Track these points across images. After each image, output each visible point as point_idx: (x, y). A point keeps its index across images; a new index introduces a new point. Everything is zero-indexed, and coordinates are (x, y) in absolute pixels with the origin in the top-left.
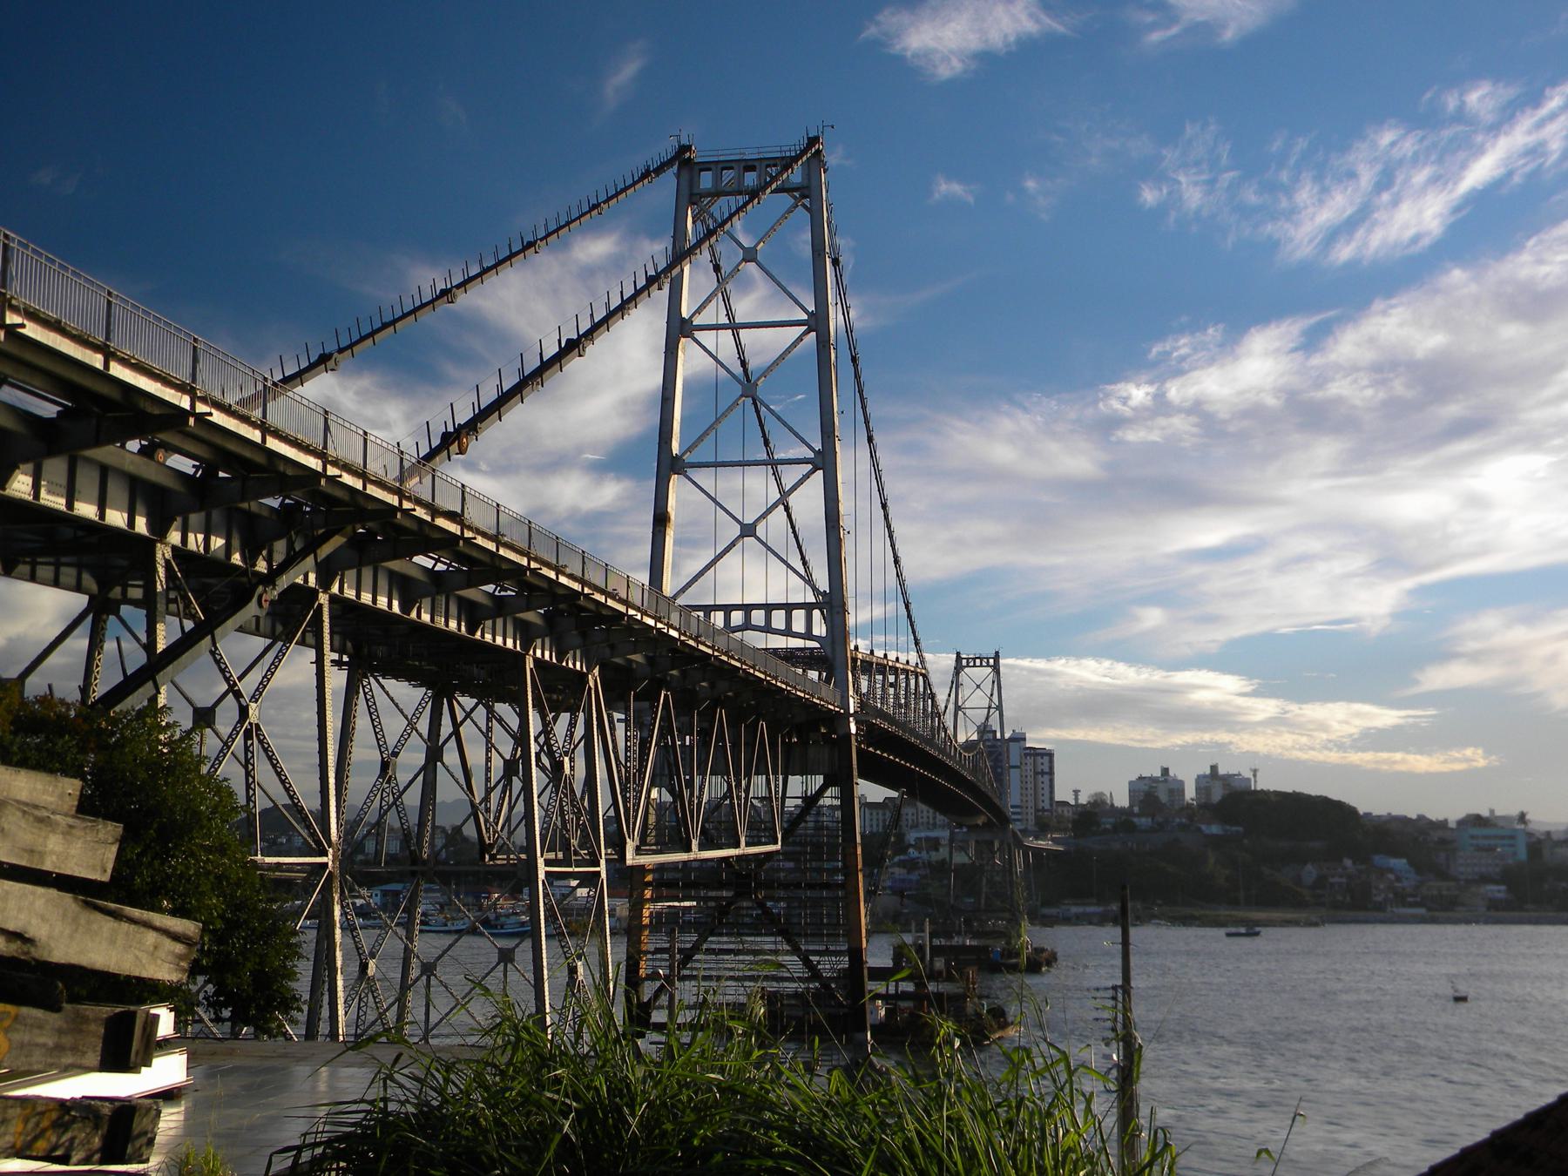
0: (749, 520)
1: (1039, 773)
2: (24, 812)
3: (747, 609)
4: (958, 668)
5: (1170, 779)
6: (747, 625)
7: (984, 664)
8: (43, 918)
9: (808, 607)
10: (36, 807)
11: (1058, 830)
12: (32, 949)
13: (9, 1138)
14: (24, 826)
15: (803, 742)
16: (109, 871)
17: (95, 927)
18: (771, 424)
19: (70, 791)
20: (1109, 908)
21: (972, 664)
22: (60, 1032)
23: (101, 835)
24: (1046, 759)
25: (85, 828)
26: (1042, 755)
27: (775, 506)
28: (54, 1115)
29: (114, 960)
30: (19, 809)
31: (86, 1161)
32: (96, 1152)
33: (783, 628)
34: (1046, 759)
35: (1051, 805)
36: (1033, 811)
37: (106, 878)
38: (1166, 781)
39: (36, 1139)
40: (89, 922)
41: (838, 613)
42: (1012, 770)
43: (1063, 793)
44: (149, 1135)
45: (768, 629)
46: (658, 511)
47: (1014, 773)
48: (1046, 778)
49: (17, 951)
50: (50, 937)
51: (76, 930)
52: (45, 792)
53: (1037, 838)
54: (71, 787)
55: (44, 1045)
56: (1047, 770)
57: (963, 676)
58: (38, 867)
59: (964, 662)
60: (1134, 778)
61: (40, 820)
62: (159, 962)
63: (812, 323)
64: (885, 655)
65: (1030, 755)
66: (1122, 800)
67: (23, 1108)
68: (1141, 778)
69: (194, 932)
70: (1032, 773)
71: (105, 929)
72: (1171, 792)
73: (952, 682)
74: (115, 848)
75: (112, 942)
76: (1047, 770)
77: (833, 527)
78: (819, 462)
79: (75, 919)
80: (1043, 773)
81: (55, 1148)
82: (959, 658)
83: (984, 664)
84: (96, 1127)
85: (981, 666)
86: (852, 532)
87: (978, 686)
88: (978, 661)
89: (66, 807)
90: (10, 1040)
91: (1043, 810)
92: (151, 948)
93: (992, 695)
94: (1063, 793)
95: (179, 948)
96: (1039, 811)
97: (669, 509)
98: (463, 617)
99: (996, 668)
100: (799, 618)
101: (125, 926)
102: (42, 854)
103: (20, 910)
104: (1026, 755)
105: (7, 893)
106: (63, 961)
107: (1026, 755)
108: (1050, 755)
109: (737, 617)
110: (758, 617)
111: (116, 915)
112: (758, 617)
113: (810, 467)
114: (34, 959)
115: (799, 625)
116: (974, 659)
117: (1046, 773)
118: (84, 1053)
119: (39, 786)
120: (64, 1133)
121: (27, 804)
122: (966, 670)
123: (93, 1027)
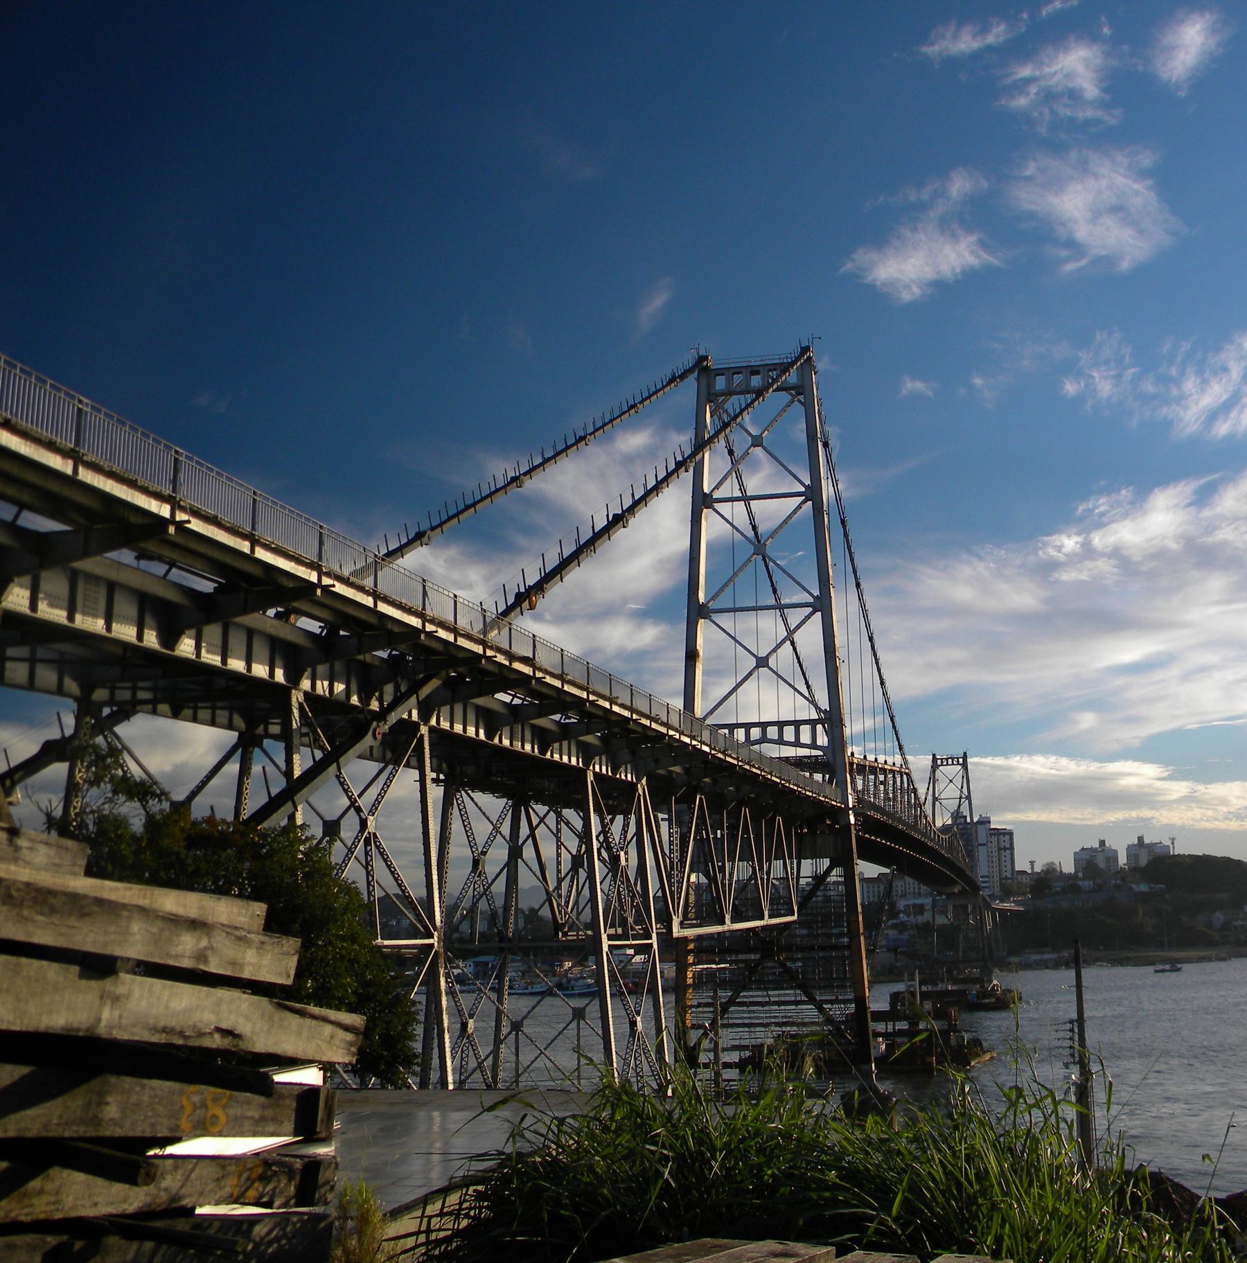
0: (762, 654)
1: (1001, 849)
2: (228, 933)
3: (764, 725)
4: (935, 767)
5: (1106, 849)
6: (764, 739)
8: (247, 1018)
9: (813, 723)
10: (236, 928)
11: (1017, 894)
12: (241, 1043)
13: (228, 1190)
14: (228, 944)
15: (812, 832)
16: (292, 977)
17: (286, 1023)
18: (778, 576)
19: (258, 913)
20: (1062, 955)
21: (945, 763)
22: (263, 1107)
23: (285, 949)
24: (1007, 837)
25: (273, 943)
26: (1004, 834)
27: (783, 642)
28: (260, 1170)
29: (301, 1049)
30: (223, 930)
31: (285, 1205)
32: (293, 1197)
33: (793, 740)
34: (1007, 837)
35: (1013, 874)
36: (998, 879)
37: (289, 982)
38: (1103, 851)
39: (247, 1190)
40: (281, 1020)
41: (837, 727)
42: (980, 847)
43: (1021, 864)
44: (331, 1183)
45: (781, 741)
46: (690, 649)
47: (982, 850)
48: (1008, 852)
49: (229, 1044)
50: (253, 1032)
51: (272, 1025)
52: (239, 914)
53: (1002, 901)
54: (260, 909)
55: (252, 1117)
56: (1008, 846)
58: (240, 976)
59: (939, 762)
61: (240, 939)
62: (335, 1048)
63: (809, 493)
64: (876, 759)
65: (994, 834)
66: (1069, 868)
67: (237, 1165)
68: (1083, 849)
69: (360, 1024)
70: (997, 849)
71: (294, 1024)
72: (1108, 859)
73: (930, 779)
74: (295, 958)
75: (299, 1034)
76: (1008, 846)
77: (831, 657)
78: (818, 605)
79: (271, 1018)
80: (1005, 849)
81: (261, 1196)
82: (934, 759)
83: (955, 763)
84: (290, 1179)
85: (953, 764)
86: (846, 661)
87: (951, 781)
88: (950, 761)
89: (255, 926)
90: (227, 1114)
91: (1006, 878)
92: (328, 1038)
93: (962, 787)
94: (1021, 864)
95: (349, 1037)
96: (1003, 879)
97: (698, 647)
98: (536, 742)
99: (965, 766)
100: (805, 731)
101: (308, 1021)
102: (242, 966)
103: (230, 1012)
104: (991, 835)
105: (220, 999)
106: (263, 1051)
107: (991, 835)
108: (1010, 834)
109: (755, 733)
110: (772, 732)
111: (302, 1013)
112: (772, 732)
113: (810, 609)
114: (242, 1050)
115: (805, 737)
116: (947, 759)
117: (1008, 849)
118: (282, 1123)
119: (235, 910)
120: (268, 1184)
121: (229, 926)
122: (941, 768)
123: (288, 1102)
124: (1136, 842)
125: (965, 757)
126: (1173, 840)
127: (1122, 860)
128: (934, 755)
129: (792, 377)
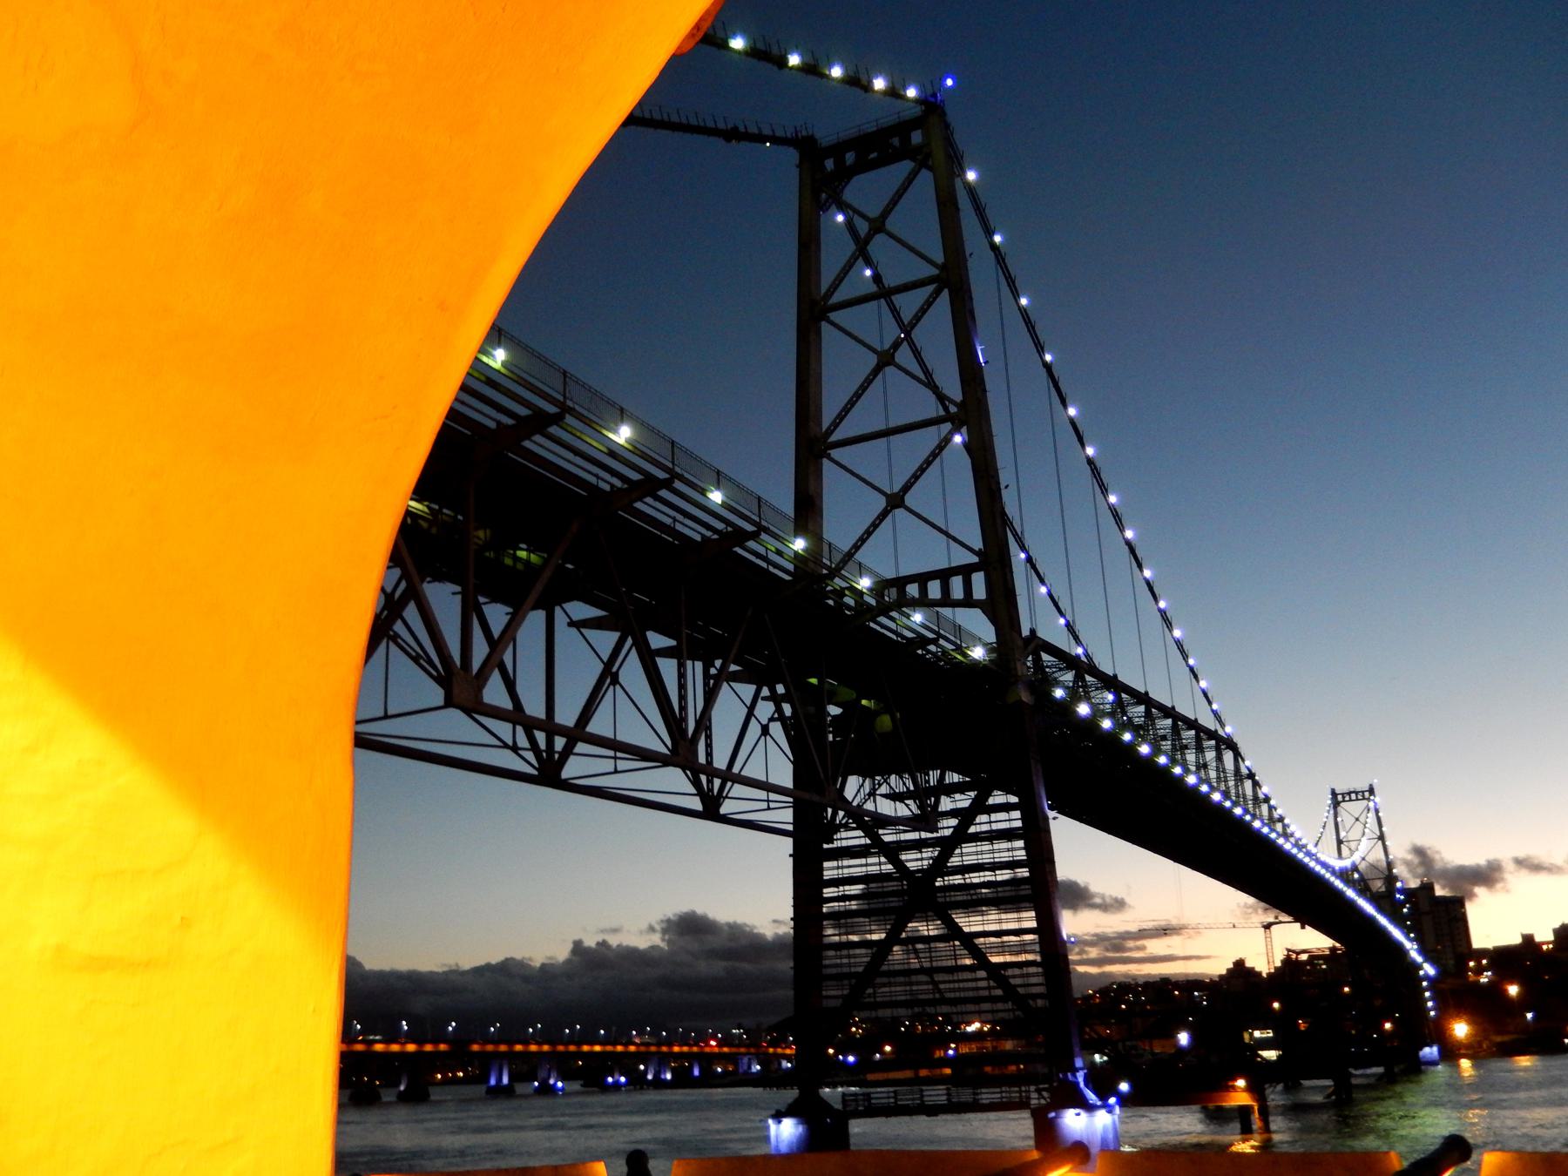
4: (1336, 804)
7: (1360, 797)
9: (966, 571)
57: (1339, 808)
59: (1340, 798)
60: (1557, 925)
82: (1334, 794)
85: (1357, 799)
86: (1013, 486)
87: (1357, 819)
88: (1353, 796)
100: (957, 583)
110: (913, 590)
115: (957, 592)
116: (1349, 793)
122: (1342, 804)
125: (1371, 791)
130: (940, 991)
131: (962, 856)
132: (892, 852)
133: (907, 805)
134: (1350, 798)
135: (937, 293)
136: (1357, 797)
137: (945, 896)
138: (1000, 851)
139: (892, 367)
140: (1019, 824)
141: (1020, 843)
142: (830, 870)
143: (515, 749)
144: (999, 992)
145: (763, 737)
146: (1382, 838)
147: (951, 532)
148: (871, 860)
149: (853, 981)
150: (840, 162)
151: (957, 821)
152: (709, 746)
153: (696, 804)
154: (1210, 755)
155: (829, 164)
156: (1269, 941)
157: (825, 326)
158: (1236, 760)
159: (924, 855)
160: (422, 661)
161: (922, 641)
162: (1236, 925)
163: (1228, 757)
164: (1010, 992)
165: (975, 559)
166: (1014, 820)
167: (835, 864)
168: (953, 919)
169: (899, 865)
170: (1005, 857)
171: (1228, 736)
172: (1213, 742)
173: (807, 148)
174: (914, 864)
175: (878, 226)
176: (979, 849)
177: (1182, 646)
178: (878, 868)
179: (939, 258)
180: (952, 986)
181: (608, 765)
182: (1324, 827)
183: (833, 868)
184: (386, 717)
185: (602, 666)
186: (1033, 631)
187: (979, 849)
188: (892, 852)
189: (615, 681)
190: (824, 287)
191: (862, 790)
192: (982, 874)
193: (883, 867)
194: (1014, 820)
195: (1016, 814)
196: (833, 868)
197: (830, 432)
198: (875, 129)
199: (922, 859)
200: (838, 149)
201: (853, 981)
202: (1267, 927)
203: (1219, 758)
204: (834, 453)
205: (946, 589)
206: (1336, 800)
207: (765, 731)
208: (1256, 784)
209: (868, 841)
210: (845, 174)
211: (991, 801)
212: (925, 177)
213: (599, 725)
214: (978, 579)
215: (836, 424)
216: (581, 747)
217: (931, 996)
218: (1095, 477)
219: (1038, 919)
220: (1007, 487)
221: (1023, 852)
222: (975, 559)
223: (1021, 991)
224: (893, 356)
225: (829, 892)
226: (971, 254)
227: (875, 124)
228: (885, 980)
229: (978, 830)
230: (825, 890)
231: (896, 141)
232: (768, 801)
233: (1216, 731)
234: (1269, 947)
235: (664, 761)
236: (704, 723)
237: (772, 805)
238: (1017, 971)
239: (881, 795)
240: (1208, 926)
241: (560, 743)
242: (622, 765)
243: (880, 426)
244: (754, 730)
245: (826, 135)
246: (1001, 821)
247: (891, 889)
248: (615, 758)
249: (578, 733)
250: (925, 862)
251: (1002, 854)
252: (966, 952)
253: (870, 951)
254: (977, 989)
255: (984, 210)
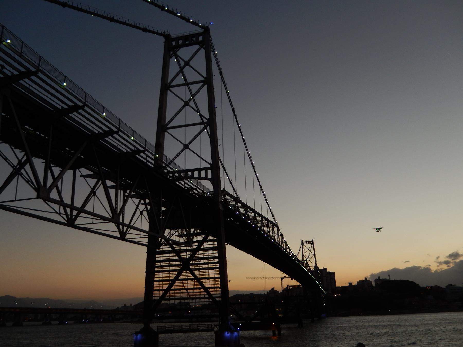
7: (309, 243)
9: (206, 169)
21: (306, 243)
45: (192, 177)
59: (304, 243)
68: (360, 281)
82: (302, 241)
83: (309, 243)
85: (309, 244)
86: (221, 145)
87: (308, 249)
88: (308, 243)
99: (313, 244)
108: (333, 274)
115: (203, 175)
116: (307, 242)
122: (304, 245)
124: (377, 278)
126: (389, 275)
127: (373, 284)
128: (302, 241)
129: (201, 38)
130: (189, 295)
131: (199, 255)
132: (178, 253)
133: (184, 239)
134: (307, 243)
135: (203, 85)
136: (308, 243)
137: (193, 267)
138: (210, 253)
139: (188, 106)
140: (216, 246)
141: (216, 252)
142: (158, 257)
143: (60, 214)
144: (207, 296)
145: (141, 215)
146: (314, 255)
147: (202, 157)
148: (171, 255)
149: (163, 292)
150: (177, 43)
151: (198, 244)
152: (123, 217)
153: (118, 235)
154: (271, 229)
155: (174, 43)
156: (282, 282)
157: (169, 92)
158: (278, 231)
159: (188, 254)
160: (30, 183)
161: (192, 189)
162: (274, 278)
163: (276, 229)
164: (210, 296)
165: (209, 166)
166: (215, 244)
167: (160, 256)
168: (195, 274)
169: (180, 257)
170: (211, 255)
171: (276, 223)
172: (272, 225)
173: (167, 37)
174: (184, 256)
175: (187, 63)
176: (204, 253)
177: (265, 197)
178: (173, 257)
179: (205, 75)
180: (193, 294)
181: (90, 221)
182: (299, 251)
183: (159, 257)
184: (16, 200)
185: (91, 189)
186: (224, 189)
187: (204, 253)
188: (178, 253)
189: (95, 194)
190: (169, 80)
191: (170, 234)
192: (204, 260)
193: (175, 257)
194: (215, 244)
195: (216, 243)
196: (159, 257)
197: (168, 124)
198: (189, 34)
199: (187, 255)
200: (177, 39)
201: (163, 292)
202: (282, 279)
203: (273, 230)
204: (169, 131)
205: (200, 174)
206: (303, 244)
207: (142, 213)
208: (283, 238)
209: (171, 249)
210: (178, 47)
211: (209, 238)
212: (203, 51)
213: (88, 208)
214: (210, 172)
215: (170, 122)
216: (82, 214)
217: (187, 297)
218: (245, 145)
219: (220, 274)
220: (220, 145)
221: (217, 254)
222: (209, 166)
223: (214, 296)
224: (189, 103)
225: (157, 264)
226: (214, 75)
227: (188, 33)
228: (173, 292)
229: (204, 247)
230: (156, 264)
231: (194, 39)
232: (141, 235)
233: (273, 222)
234: (282, 285)
235: (109, 220)
236: (122, 210)
237: (142, 236)
238: (213, 290)
239: (176, 235)
240: (268, 278)
241: (75, 213)
242: (95, 221)
243: (183, 124)
244: (138, 213)
245: (173, 34)
246: (211, 245)
247: (176, 264)
248: (93, 219)
249: (81, 210)
250: (188, 256)
251: (211, 255)
252: (198, 284)
253: (169, 283)
254: (201, 295)
255: (219, 63)
